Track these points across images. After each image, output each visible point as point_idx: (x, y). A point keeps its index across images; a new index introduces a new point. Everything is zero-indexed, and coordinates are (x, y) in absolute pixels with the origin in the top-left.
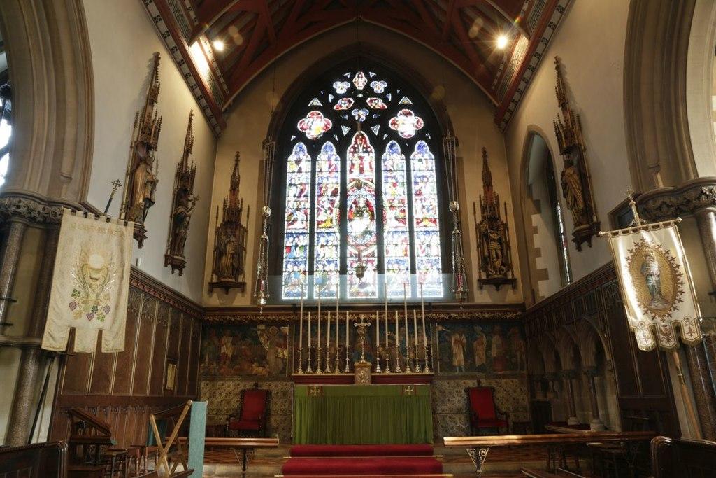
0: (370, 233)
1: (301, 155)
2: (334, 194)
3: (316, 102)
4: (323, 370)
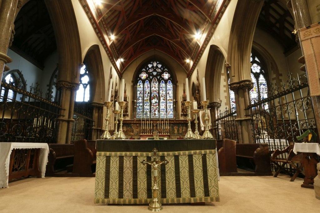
0: (157, 103)
1: (140, 83)
2: (148, 93)
3: (144, 70)
4: (146, 134)
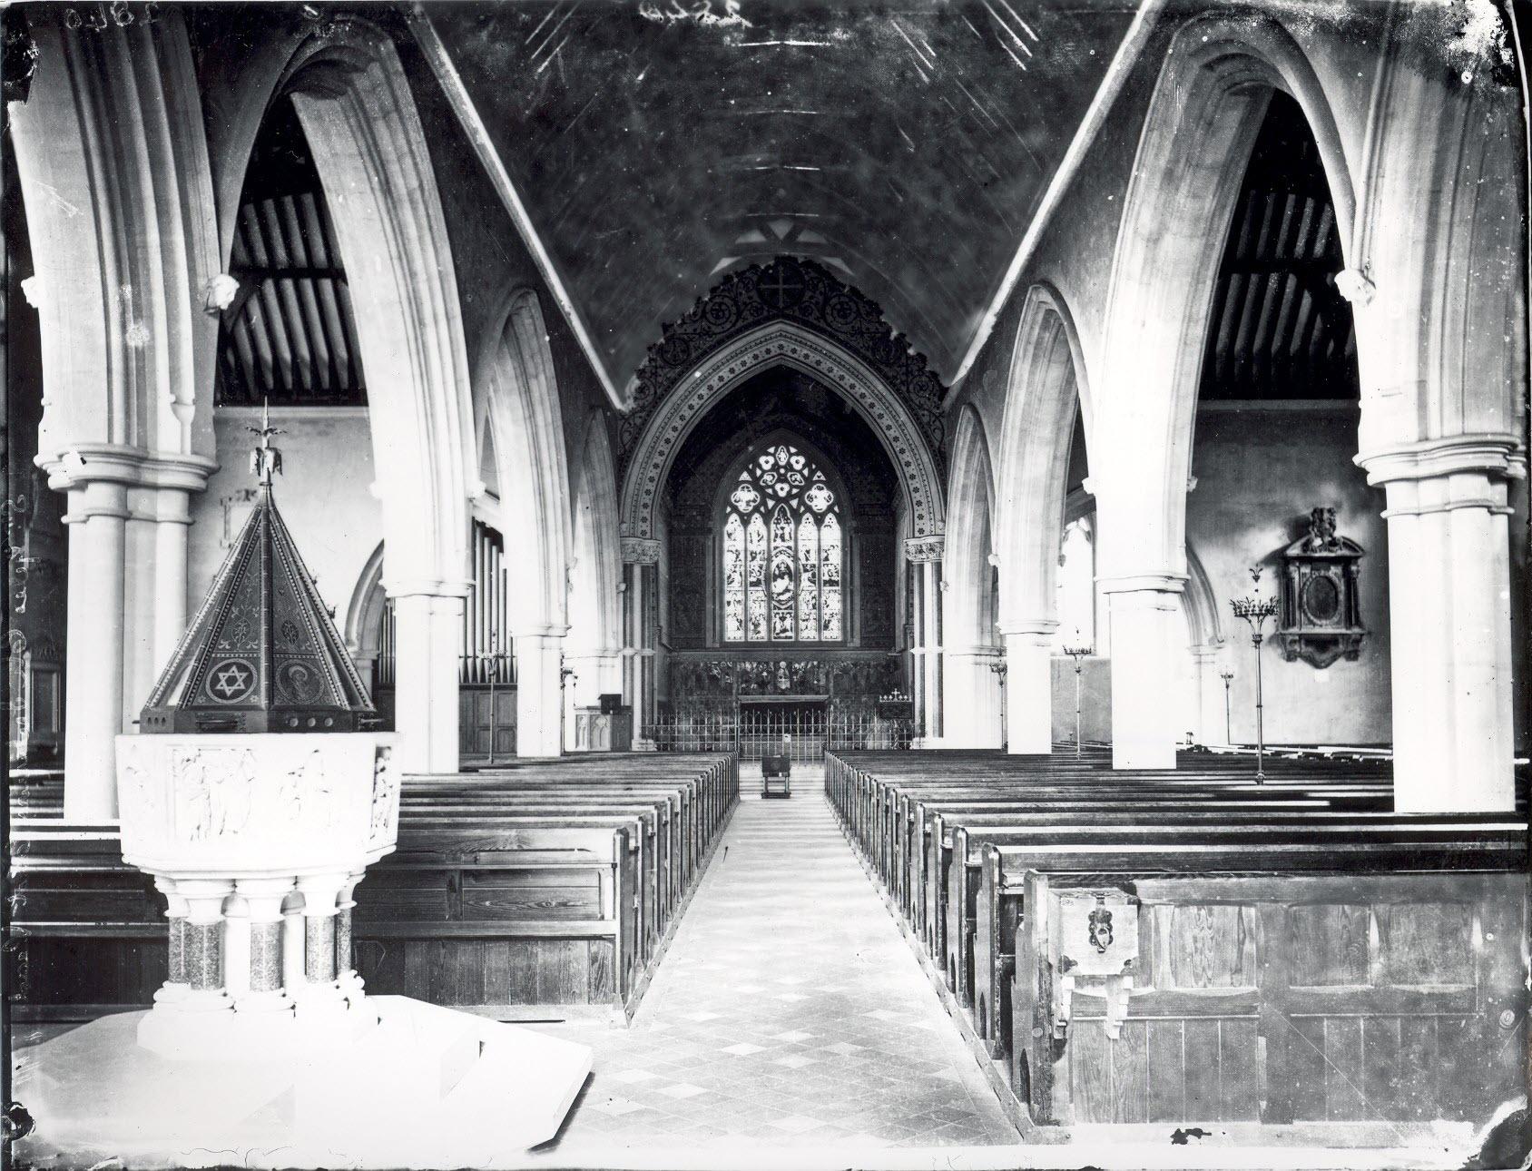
3: (745, 476)
